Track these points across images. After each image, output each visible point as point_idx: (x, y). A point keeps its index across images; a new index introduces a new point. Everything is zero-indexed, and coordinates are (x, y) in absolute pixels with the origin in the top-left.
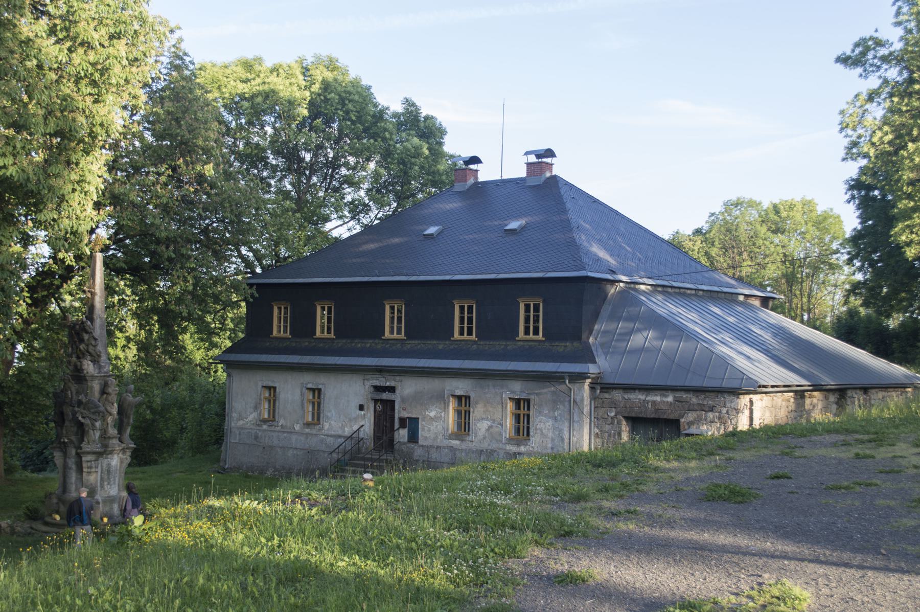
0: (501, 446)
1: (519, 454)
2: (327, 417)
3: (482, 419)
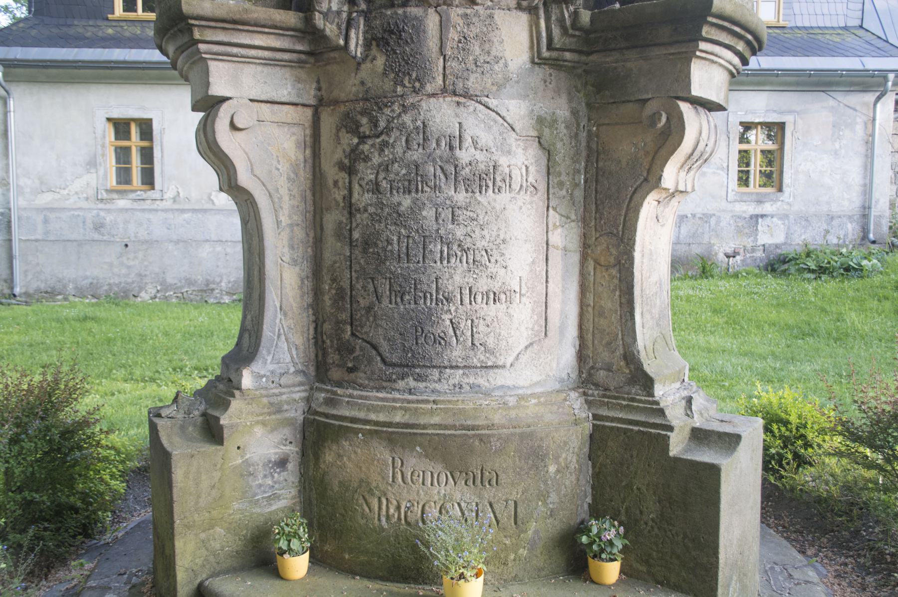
0: (724, 205)
1: (762, 216)
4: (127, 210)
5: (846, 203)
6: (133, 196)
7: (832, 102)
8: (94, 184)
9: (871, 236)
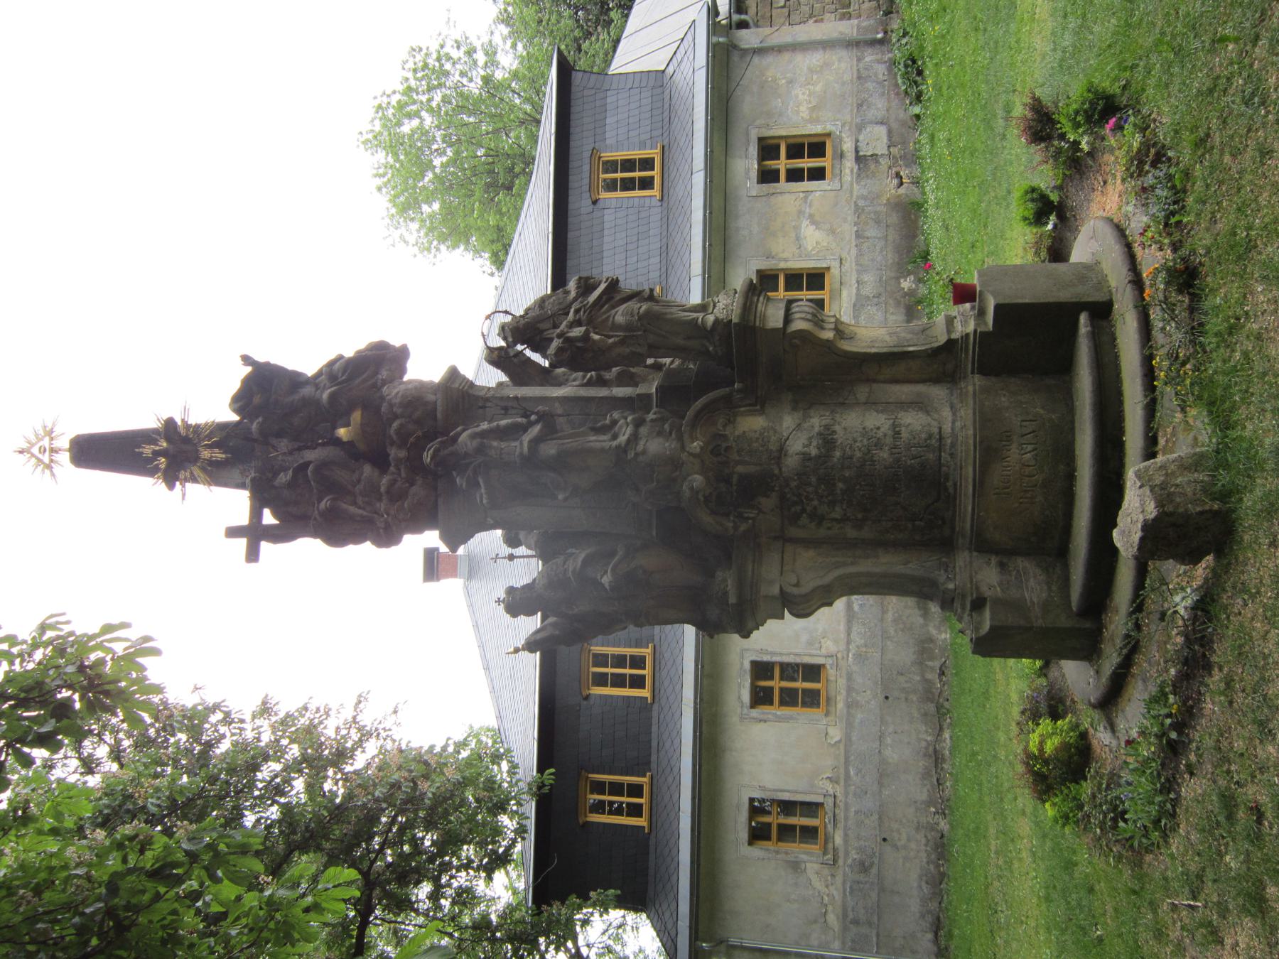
1: (857, 151)
2: (810, 643)
3: (798, 238)
4: (846, 835)
5: (843, 65)
6: (830, 828)
7: (738, 92)
8: (816, 866)
9: (880, 36)
